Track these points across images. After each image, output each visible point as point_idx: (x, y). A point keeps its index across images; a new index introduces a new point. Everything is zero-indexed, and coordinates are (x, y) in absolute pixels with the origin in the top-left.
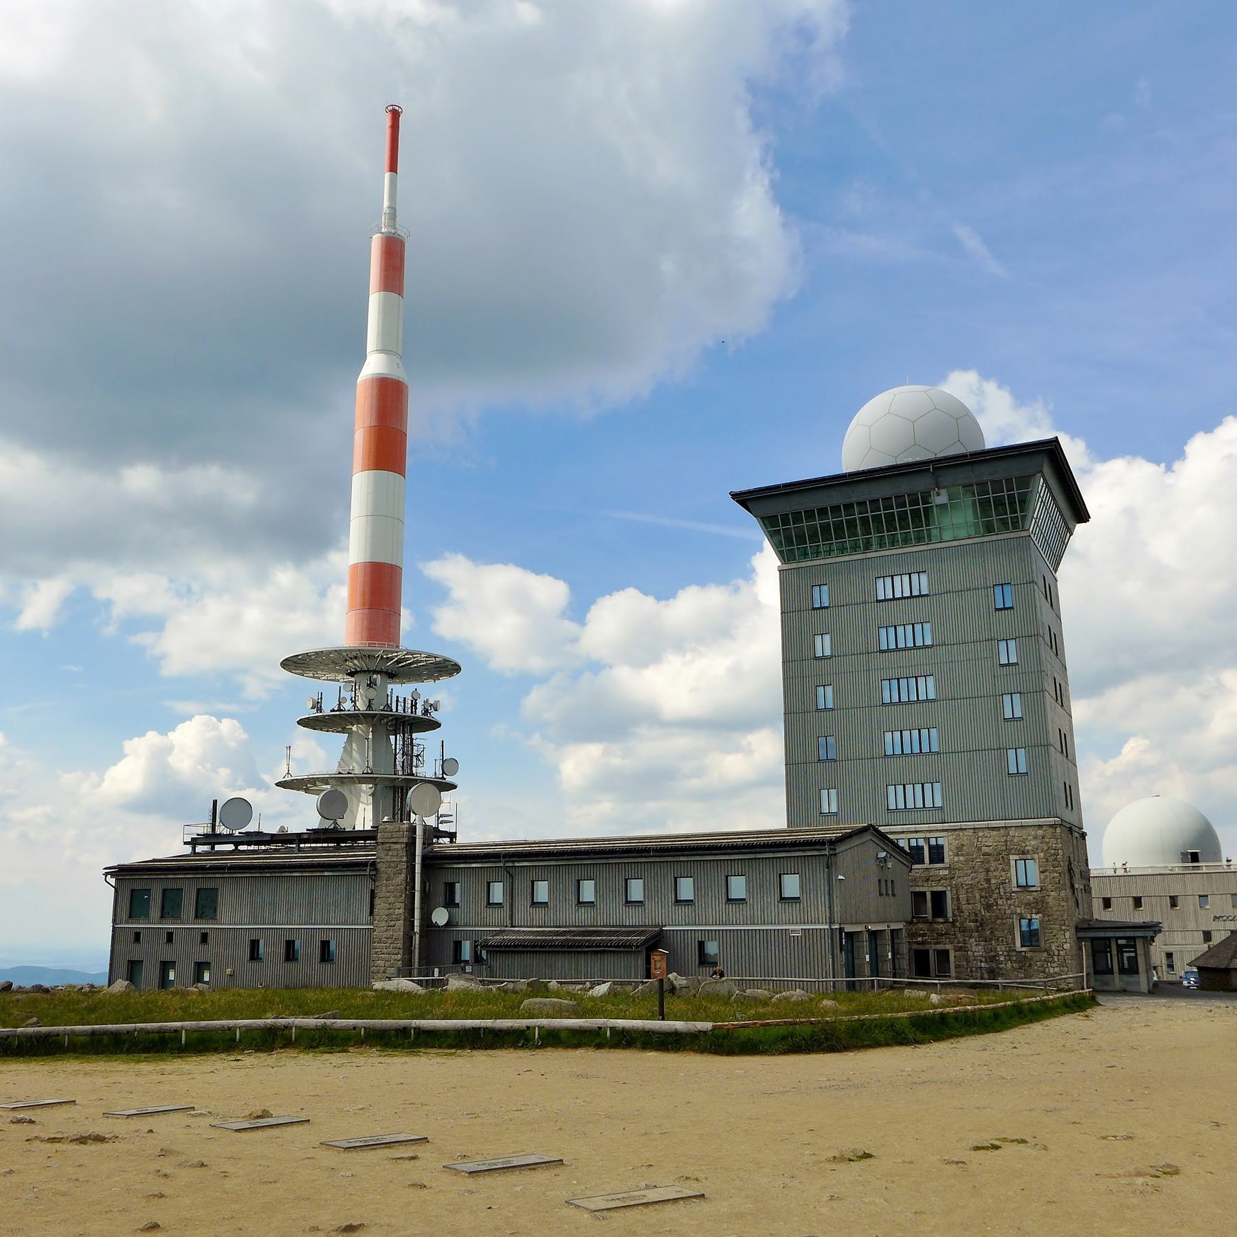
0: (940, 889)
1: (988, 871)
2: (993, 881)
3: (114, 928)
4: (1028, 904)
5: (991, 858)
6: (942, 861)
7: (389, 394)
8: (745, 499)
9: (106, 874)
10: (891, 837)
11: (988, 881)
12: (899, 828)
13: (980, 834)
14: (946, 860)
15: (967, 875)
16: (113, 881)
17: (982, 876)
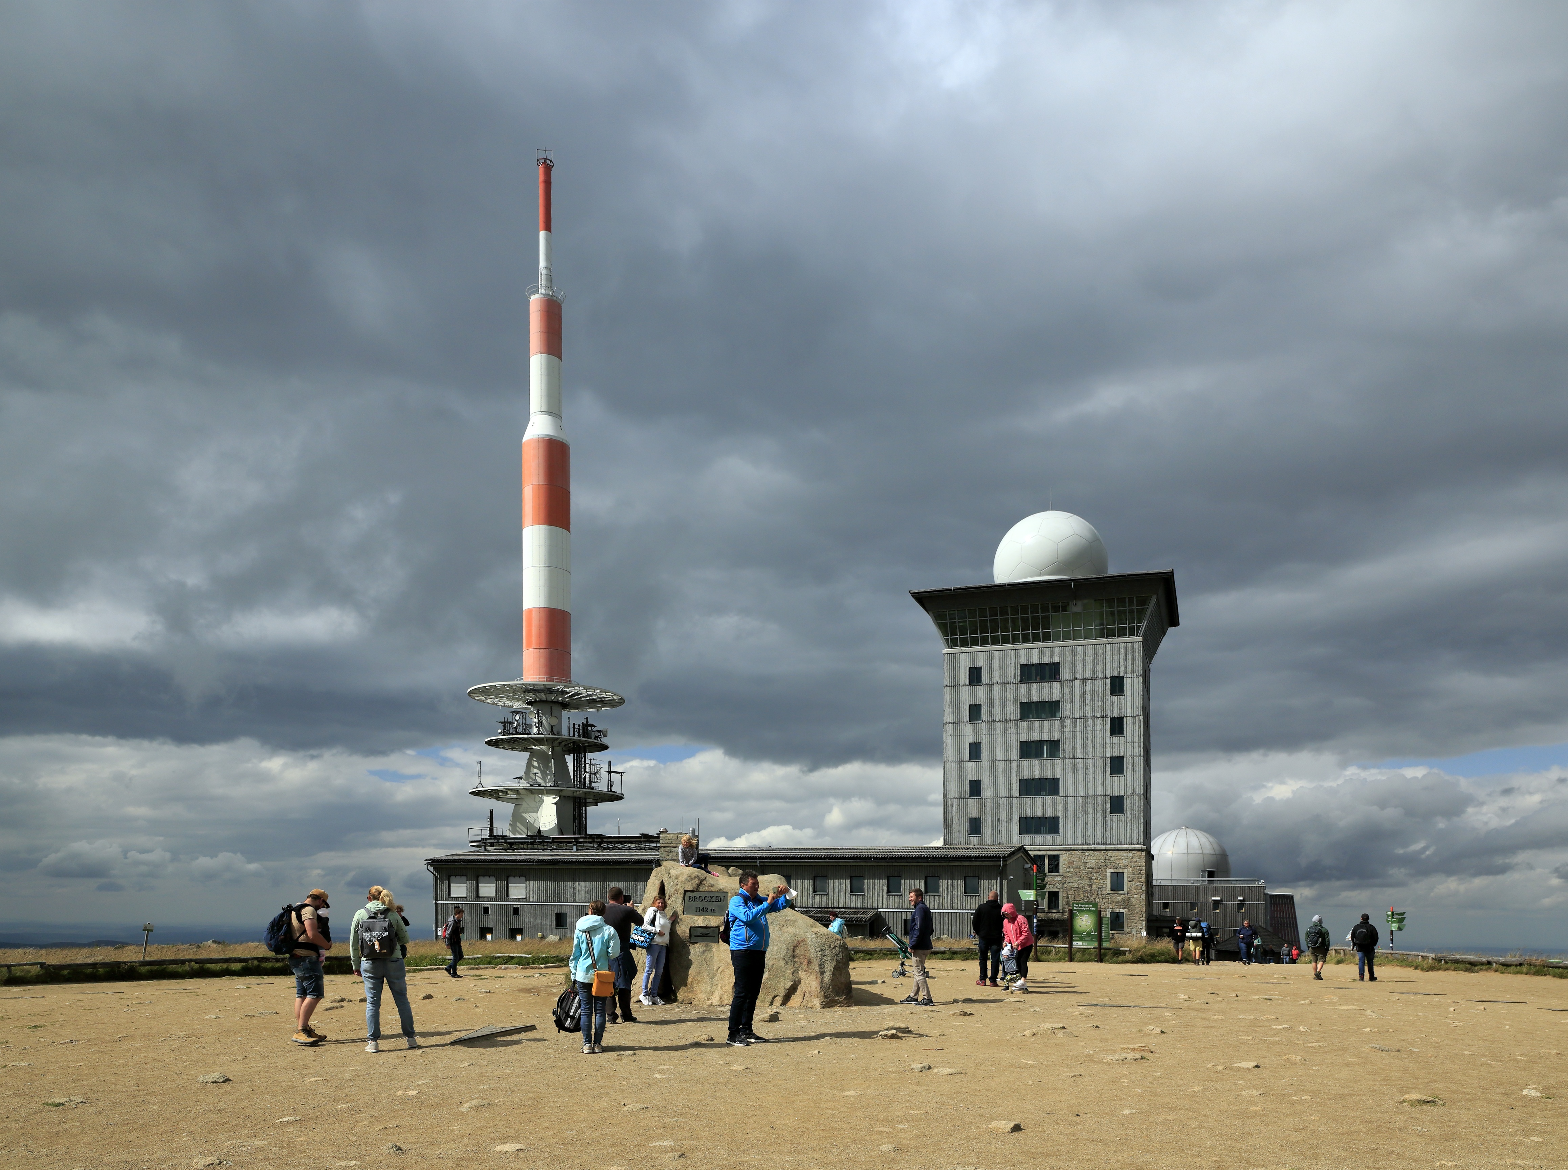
0: (1056, 890)
1: (1091, 878)
2: (1094, 886)
3: (436, 904)
4: (1118, 902)
5: (1094, 871)
6: (1058, 871)
7: (556, 453)
8: (924, 599)
9: (428, 864)
10: (1030, 853)
11: (1091, 886)
12: (1038, 847)
13: (1087, 853)
14: (1061, 871)
15: (1075, 881)
16: (432, 869)
17: (1086, 882)
